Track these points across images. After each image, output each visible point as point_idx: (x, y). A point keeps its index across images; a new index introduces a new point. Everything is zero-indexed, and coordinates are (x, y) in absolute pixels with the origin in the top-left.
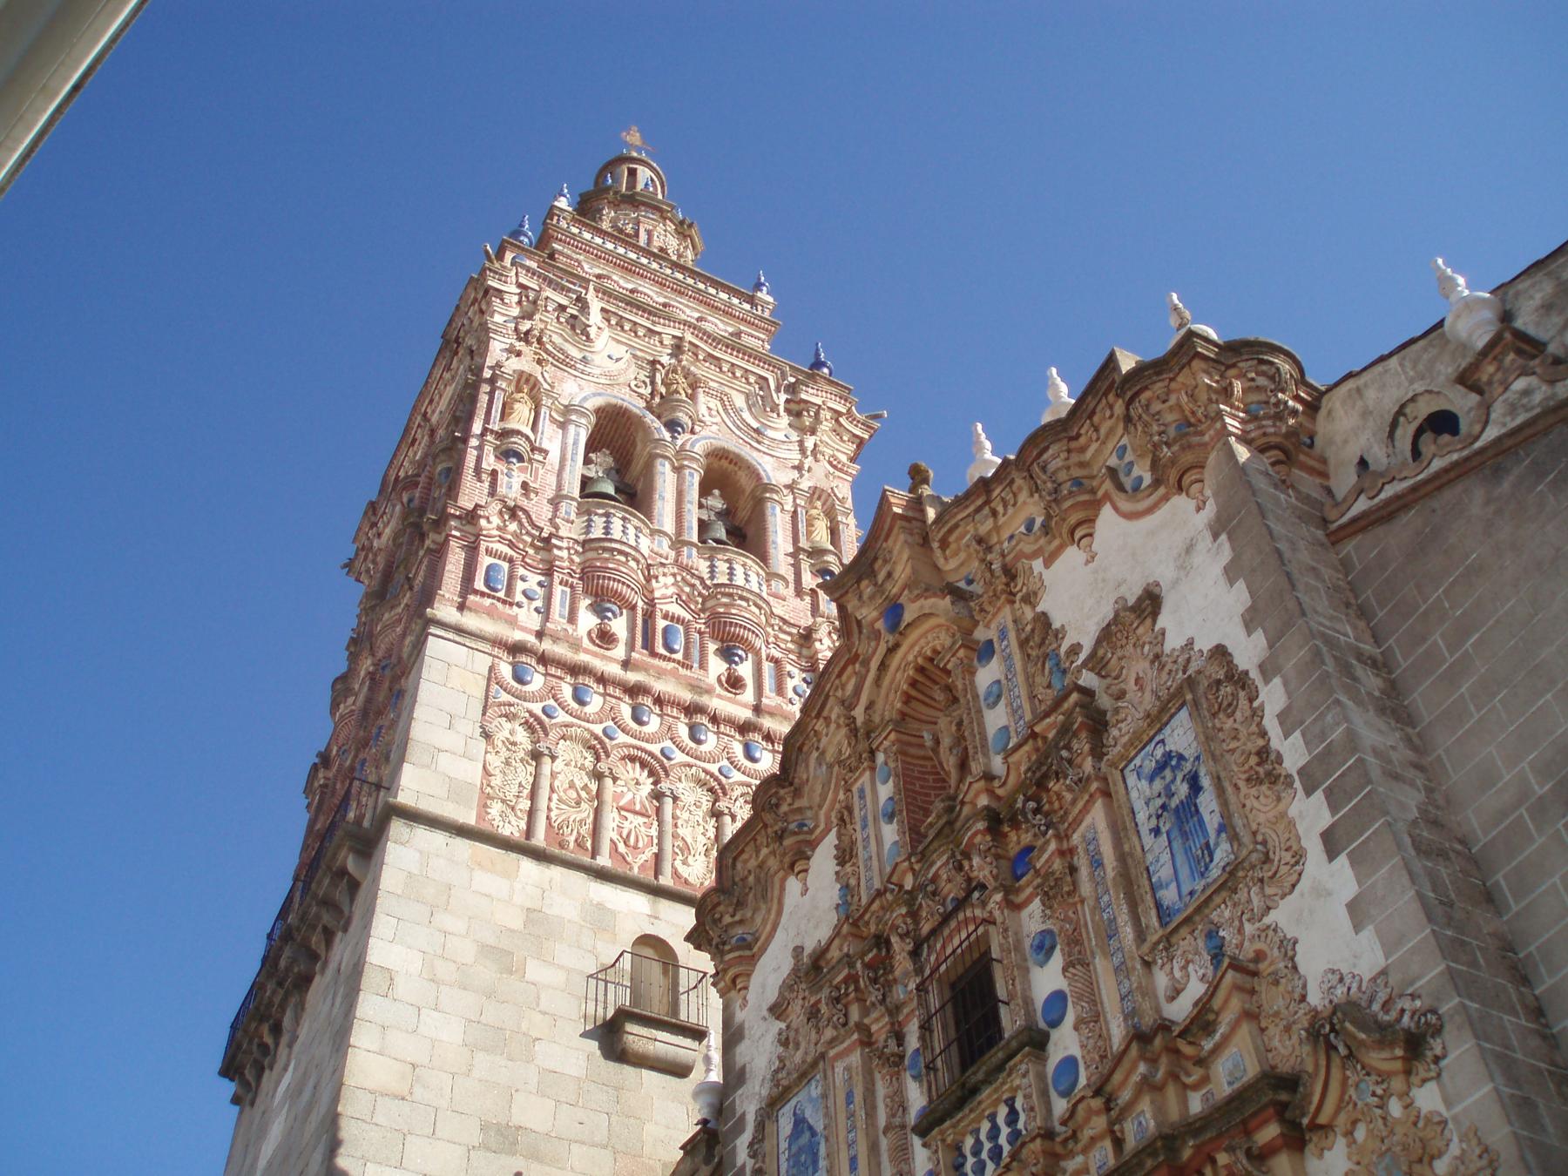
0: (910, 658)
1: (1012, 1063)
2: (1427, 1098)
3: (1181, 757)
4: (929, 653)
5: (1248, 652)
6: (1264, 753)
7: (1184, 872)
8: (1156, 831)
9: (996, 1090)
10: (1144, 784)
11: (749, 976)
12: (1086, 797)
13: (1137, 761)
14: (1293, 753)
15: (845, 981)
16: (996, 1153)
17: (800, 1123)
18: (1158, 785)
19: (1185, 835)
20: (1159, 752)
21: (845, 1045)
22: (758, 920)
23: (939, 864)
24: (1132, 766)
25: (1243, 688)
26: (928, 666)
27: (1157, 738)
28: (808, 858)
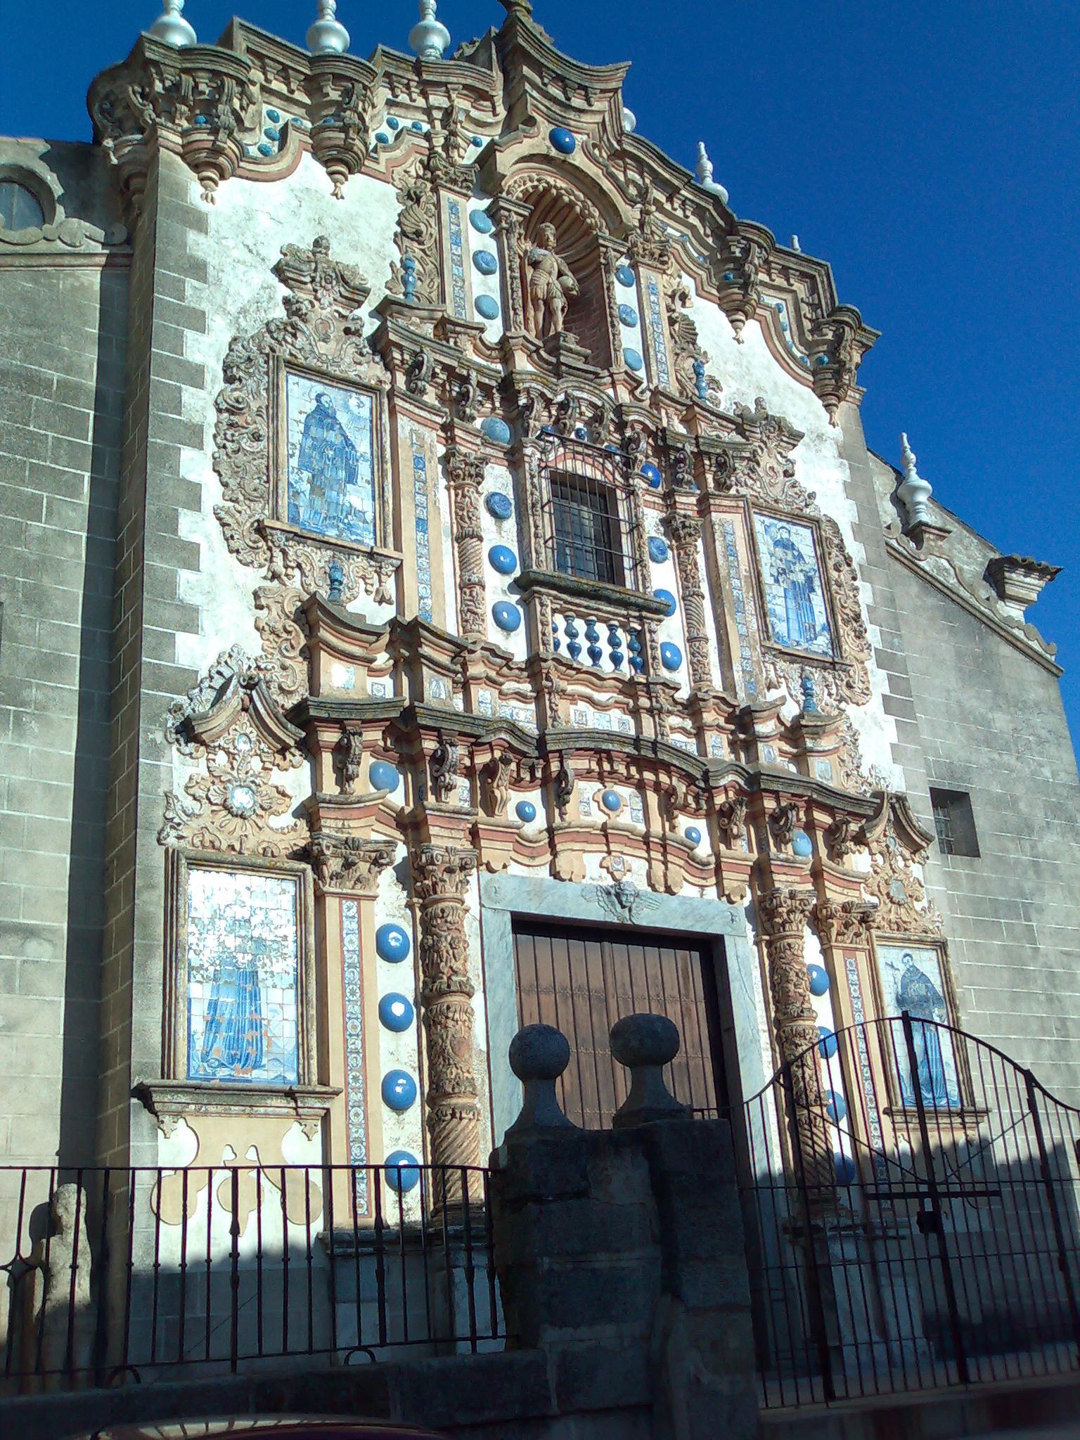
0: (551, 181)
1: (649, 615)
2: (916, 870)
3: (800, 557)
4: (566, 199)
5: (855, 549)
6: (857, 617)
7: (794, 625)
8: (777, 581)
9: (614, 614)
10: (771, 542)
11: (222, 177)
12: (733, 504)
13: (768, 521)
14: (873, 635)
15: (446, 368)
16: (595, 655)
17: (322, 416)
18: (779, 552)
19: (799, 607)
20: (785, 536)
21: (423, 413)
22: (247, 139)
23: (585, 395)
24: (763, 518)
25: (849, 565)
26: (547, 200)
27: (784, 524)
28: (351, 172)
